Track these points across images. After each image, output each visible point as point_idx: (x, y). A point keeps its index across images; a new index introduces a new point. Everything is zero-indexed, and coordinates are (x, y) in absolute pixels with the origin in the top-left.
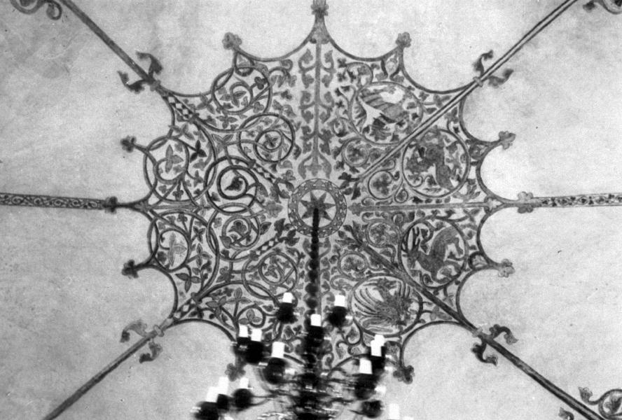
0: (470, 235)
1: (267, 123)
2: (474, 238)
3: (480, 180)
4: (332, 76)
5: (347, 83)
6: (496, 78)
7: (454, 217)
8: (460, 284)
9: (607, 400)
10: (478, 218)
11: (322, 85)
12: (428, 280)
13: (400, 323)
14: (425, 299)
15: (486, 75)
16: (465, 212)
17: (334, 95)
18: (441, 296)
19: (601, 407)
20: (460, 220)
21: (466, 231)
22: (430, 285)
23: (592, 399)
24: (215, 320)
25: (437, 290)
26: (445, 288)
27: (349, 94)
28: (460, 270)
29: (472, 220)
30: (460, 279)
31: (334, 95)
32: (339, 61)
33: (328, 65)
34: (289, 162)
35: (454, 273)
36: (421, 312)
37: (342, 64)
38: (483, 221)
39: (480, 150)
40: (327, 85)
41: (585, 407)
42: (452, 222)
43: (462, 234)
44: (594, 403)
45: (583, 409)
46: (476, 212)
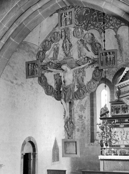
0: (106, 27)
2: (106, 28)
3: (121, 26)
7: (110, 22)
8: (94, 28)
10: (111, 27)
12: (92, 20)
13: (79, 23)
14: (87, 22)
16: (112, 24)
18: (89, 25)
20: (110, 23)
21: (108, 25)
22: (91, 21)
25: (90, 23)
26: (92, 25)
28: (97, 27)
29: (111, 26)
30: (95, 28)
35: (96, 26)
36: (84, 24)
38: (111, 28)
42: (109, 21)
43: (106, 24)
46: (113, 26)
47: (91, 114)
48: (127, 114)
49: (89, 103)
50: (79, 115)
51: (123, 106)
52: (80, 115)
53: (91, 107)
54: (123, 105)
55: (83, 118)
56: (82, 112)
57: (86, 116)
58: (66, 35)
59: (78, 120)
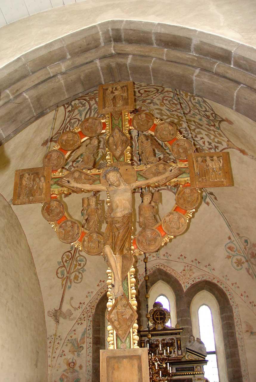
1: (185, 107)
4: (210, 139)
5: (207, 144)
6: (206, 199)
9: (82, 257)
11: (207, 133)
15: (208, 195)
17: (201, 136)
19: (78, 256)
23: (80, 252)
24: (67, 114)
27: (201, 142)
31: (201, 136)
32: (218, 146)
33: (216, 140)
34: (164, 106)
37: (216, 147)
39: (174, 189)
40: (206, 135)
41: (77, 252)
44: (79, 254)
45: (75, 252)
47: (93, 358)
48: (174, 356)
49: (91, 336)
50: (68, 361)
51: (164, 340)
52: (71, 361)
53: (93, 343)
54: (164, 337)
55: (77, 368)
56: (74, 354)
57: (84, 365)
58: (116, 122)
59: (65, 373)
